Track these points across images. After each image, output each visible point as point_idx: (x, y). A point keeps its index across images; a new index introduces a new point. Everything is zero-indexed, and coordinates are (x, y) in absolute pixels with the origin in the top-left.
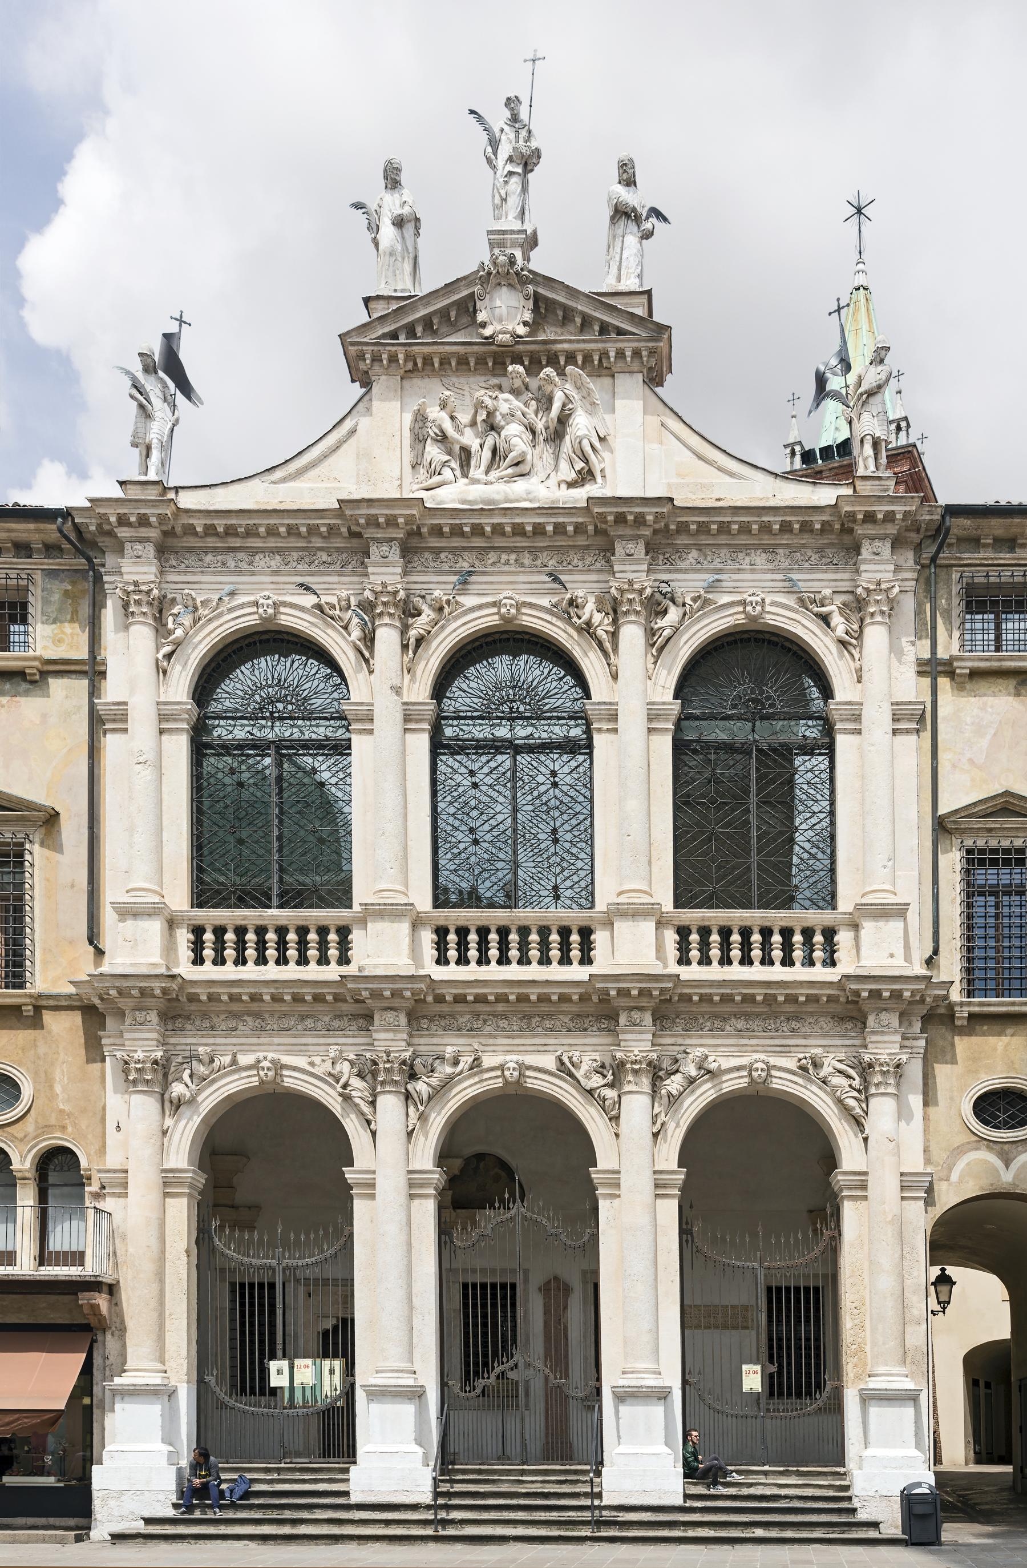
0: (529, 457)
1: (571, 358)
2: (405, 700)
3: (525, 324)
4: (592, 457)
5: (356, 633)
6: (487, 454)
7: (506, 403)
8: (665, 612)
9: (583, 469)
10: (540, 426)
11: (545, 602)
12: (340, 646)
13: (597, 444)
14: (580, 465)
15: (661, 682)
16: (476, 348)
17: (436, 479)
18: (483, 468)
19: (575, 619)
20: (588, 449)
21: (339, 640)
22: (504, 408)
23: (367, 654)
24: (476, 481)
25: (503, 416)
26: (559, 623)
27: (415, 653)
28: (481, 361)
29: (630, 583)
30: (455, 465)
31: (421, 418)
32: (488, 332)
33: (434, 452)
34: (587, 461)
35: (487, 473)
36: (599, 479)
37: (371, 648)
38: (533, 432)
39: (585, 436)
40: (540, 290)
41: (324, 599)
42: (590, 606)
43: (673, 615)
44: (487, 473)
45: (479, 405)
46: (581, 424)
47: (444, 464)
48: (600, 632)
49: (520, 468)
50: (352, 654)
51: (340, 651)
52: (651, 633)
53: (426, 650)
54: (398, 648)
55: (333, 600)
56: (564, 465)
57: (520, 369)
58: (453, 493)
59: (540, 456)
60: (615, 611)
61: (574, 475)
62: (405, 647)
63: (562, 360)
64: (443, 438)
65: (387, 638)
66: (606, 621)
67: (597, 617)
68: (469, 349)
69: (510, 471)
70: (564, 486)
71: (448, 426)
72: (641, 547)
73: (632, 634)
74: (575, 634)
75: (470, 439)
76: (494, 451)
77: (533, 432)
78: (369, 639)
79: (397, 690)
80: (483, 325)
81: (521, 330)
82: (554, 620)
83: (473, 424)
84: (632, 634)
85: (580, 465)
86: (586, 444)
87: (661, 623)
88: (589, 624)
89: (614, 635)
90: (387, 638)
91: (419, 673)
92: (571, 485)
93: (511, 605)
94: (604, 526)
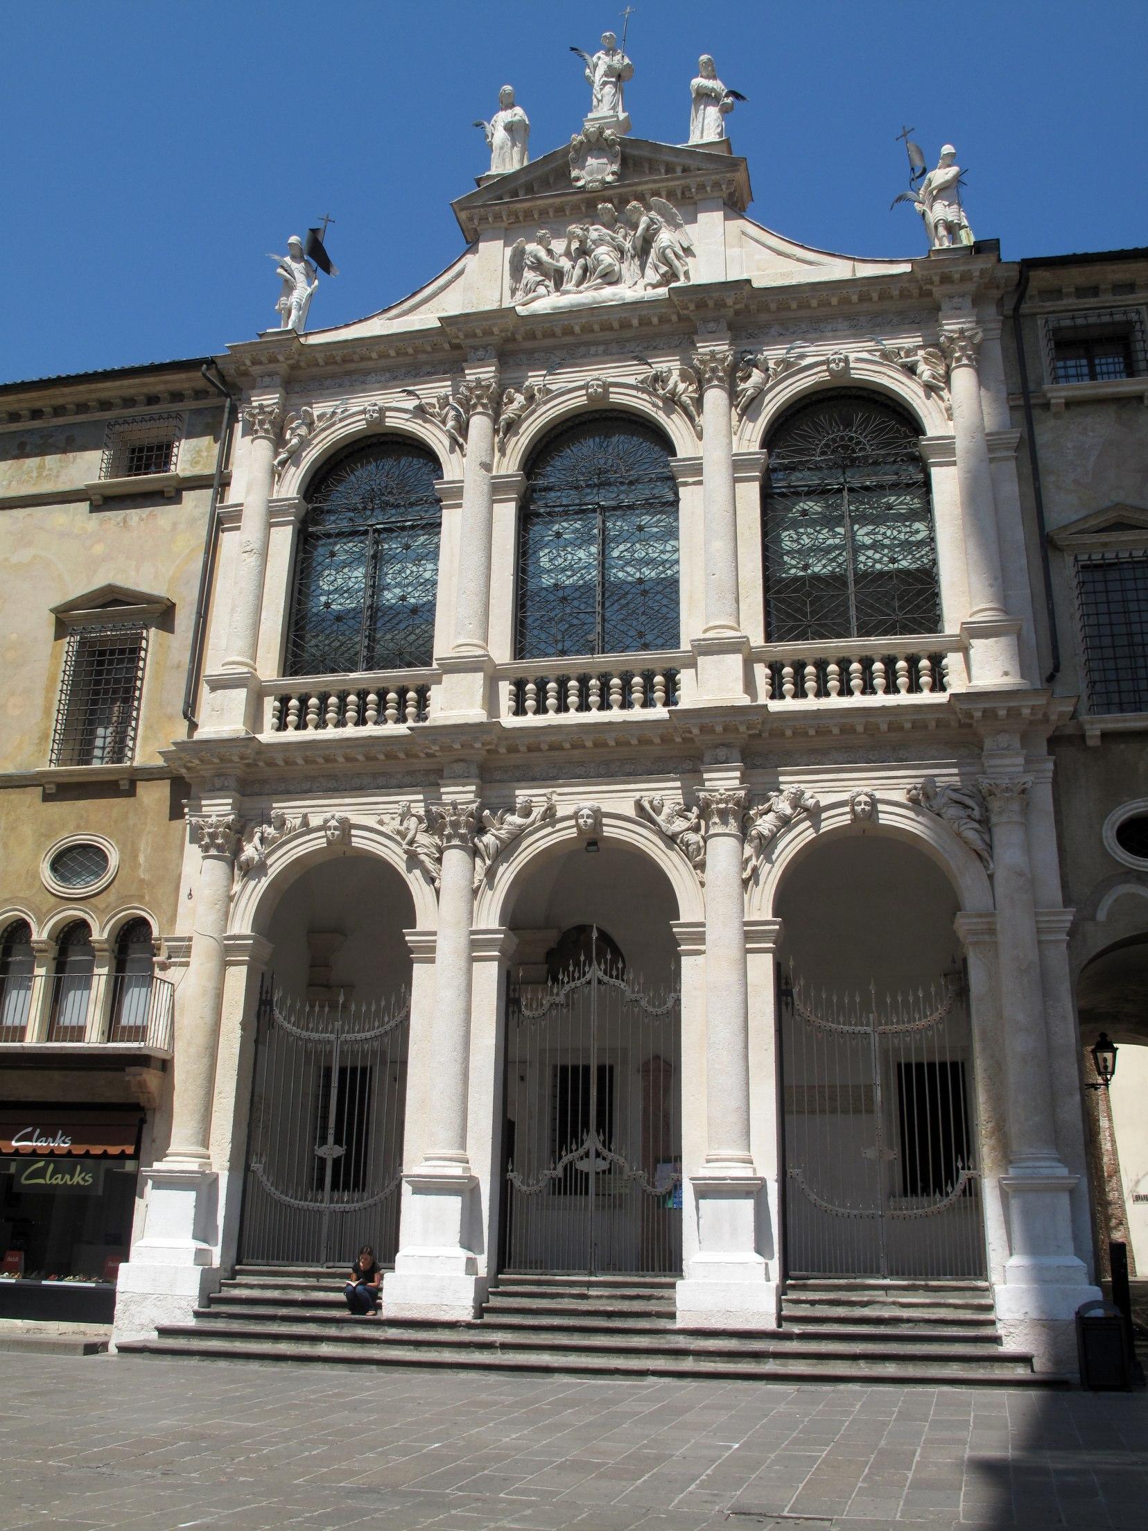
0: (616, 268)
1: (656, 193)
2: (494, 473)
3: (613, 173)
4: (676, 262)
5: (451, 423)
6: (578, 272)
7: (596, 231)
8: (750, 376)
9: (666, 272)
10: (628, 245)
11: (631, 380)
12: (435, 437)
13: (681, 253)
14: (663, 269)
15: (747, 436)
16: (569, 198)
17: (532, 295)
18: (574, 282)
19: (661, 392)
20: (672, 256)
21: (437, 432)
22: (594, 235)
23: (461, 440)
24: (568, 292)
25: (594, 242)
26: (645, 396)
27: (505, 435)
28: (575, 208)
29: (713, 354)
30: (551, 284)
31: (519, 255)
32: (580, 184)
33: (529, 276)
34: (670, 265)
35: (578, 286)
36: (682, 278)
37: (465, 438)
38: (622, 252)
39: (669, 247)
40: (628, 150)
41: (424, 401)
42: (675, 376)
43: (757, 376)
44: (579, 284)
45: (571, 237)
46: (665, 237)
47: (538, 283)
48: (684, 398)
49: (610, 278)
50: (447, 442)
51: (436, 441)
52: (733, 395)
53: (516, 433)
54: (490, 431)
55: (434, 401)
56: (649, 271)
57: (610, 206)
58: (547, 302)
59: (629, 269)
60: (700, 382)
61: (658, 277)
62: (496, 431)
63: (647, 196)
64: (538, 266)
65: (479, 425)
66: (691, 389)
67: (681, 387)
68: (564, 199)
69: (599, 281)
70: (649, 288)
71: (543, 254)
72: (724, 325)
73: (715, 398)
74: (661, 404)
75: (565, 263)
76: (585, 269)
77: (622, 252)
78: (463, 428)
79: (487, 467)
80: (578, 179)
81: (609, 178)
82: (639, 394)
83: (567, 254)
84: (715, 398)
85: (663, 269)
86: (668, 251)
87: (742, 386)
88: (673, 392)
89: (699, 402)
90: (479, 425)
91: (508, 452)
92: (654, 286)
93: (598, 386)
94: (686, 312)
